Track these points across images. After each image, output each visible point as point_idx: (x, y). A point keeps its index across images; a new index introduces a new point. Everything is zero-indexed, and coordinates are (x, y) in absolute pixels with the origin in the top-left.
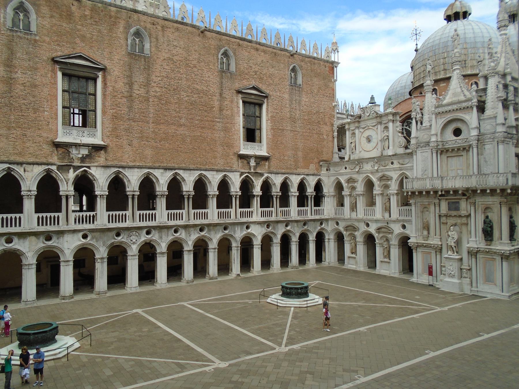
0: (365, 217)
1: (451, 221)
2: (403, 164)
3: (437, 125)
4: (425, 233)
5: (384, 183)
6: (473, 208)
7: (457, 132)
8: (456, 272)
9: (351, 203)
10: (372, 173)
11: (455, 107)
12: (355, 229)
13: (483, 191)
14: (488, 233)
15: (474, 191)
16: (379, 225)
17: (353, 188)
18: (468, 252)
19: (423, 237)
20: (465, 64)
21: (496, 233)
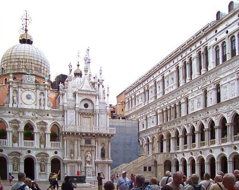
0: (26, 147)
1: (86, 149)
2: (55, 117)
3: (79, 99)
4: (72, 155)
5: (41, 126)
6: (97, 143)
7: (86, 106)
8: (91, 174)
9: (13, 136)
10: (32, 119)
11: (89, 93)
12: (19, 154)
13: (104, 135)
14: (103, 155)
15: (100, 135)
16: (39, 152)
17: (16, 128)
18: (95, 164)
19: (71, 158)
20: (41, 71)
21: (106, 155)
